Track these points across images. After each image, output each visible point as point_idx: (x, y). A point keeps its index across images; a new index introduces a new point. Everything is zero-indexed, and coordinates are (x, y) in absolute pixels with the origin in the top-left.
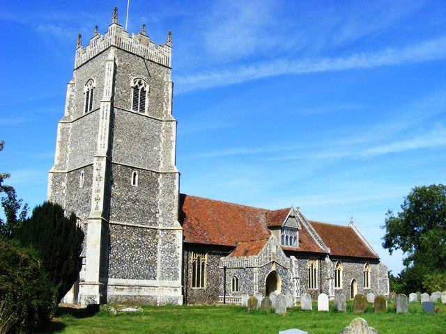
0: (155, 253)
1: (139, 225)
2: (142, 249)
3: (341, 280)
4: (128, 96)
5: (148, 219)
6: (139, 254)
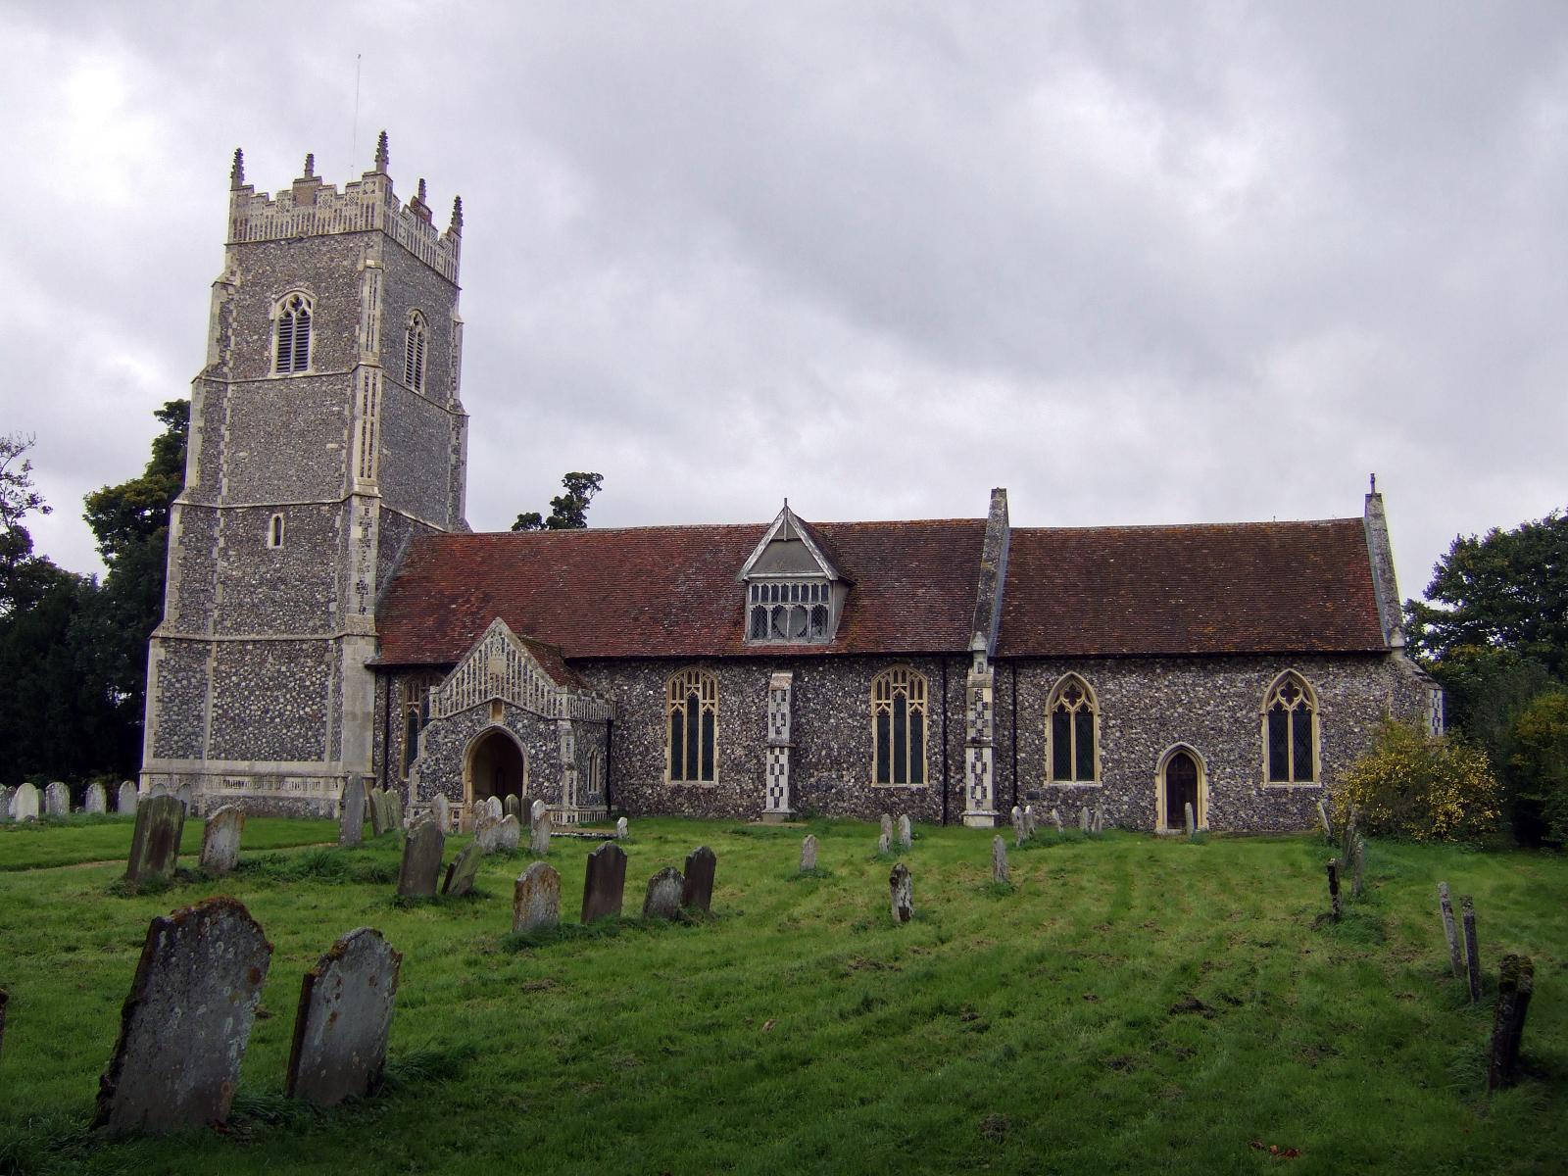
0: (322, 697)
1: (285, 636)
2: (289, 691)
3: (1099, 752)
4: (265, 347)
5: (307, 620)
6: (285, 704)
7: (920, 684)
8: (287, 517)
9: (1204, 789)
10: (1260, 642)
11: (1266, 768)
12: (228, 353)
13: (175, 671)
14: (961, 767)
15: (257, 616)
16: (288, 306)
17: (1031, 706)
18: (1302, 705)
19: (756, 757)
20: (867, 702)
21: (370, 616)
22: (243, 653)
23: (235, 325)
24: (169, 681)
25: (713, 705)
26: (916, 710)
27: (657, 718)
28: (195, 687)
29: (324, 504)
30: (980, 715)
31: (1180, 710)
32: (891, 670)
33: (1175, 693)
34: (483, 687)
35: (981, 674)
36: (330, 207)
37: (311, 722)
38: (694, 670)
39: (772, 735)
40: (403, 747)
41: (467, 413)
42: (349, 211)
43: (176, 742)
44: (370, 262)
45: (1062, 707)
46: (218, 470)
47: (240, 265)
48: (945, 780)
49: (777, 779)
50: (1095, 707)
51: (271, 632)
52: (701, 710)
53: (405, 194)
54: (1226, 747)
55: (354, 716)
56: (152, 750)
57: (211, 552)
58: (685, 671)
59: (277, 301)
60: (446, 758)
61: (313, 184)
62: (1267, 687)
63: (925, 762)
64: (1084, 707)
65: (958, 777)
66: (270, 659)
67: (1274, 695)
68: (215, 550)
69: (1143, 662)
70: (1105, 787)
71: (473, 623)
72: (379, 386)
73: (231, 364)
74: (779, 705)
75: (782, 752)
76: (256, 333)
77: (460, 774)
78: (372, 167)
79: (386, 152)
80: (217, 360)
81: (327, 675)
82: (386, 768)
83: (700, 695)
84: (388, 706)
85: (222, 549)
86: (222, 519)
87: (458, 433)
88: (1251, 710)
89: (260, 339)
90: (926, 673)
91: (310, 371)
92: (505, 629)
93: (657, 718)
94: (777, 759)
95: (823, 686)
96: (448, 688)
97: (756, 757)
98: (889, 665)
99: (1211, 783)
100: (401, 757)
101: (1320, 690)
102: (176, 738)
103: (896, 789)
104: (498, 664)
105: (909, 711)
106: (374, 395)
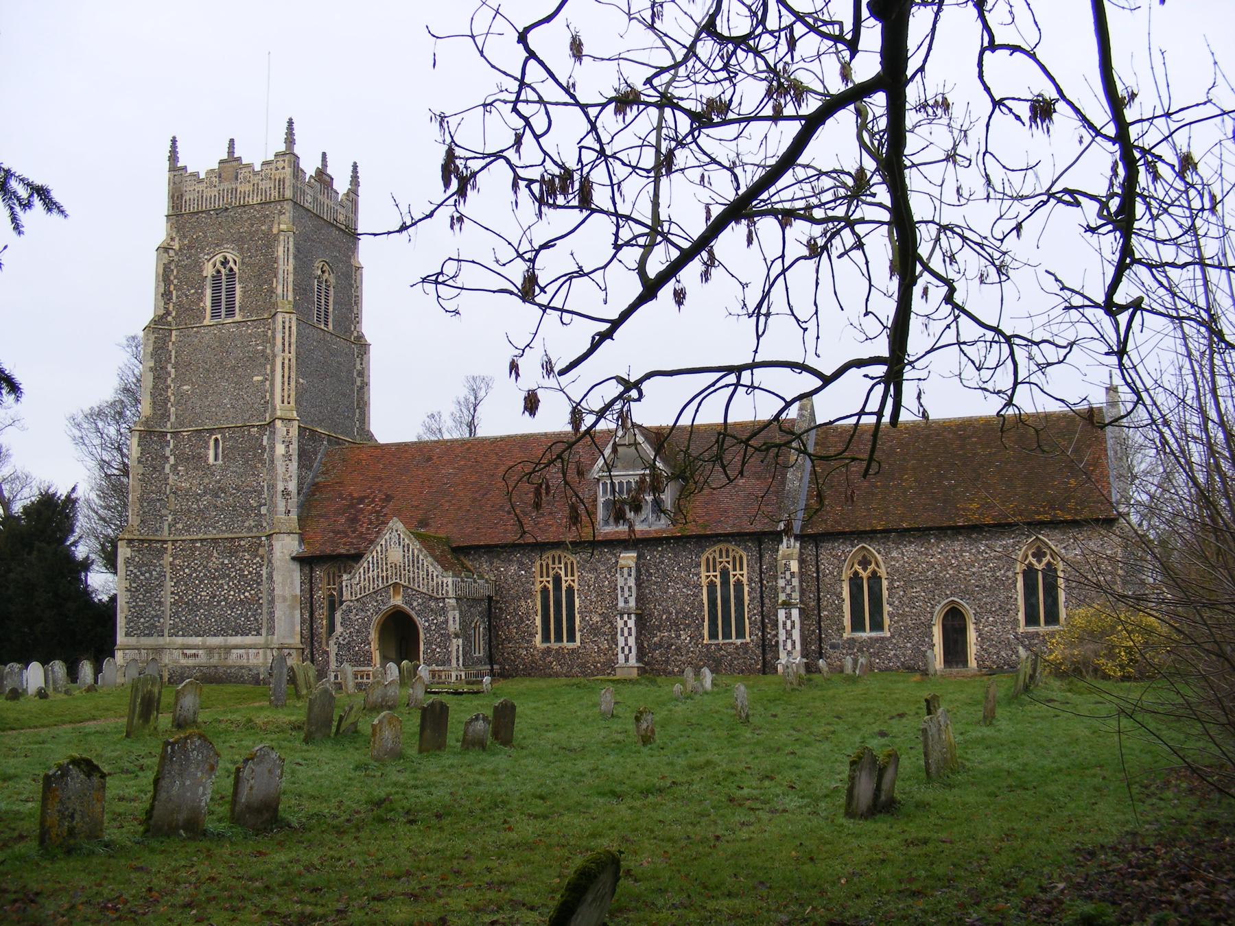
0: (258, 584)
1: (226, 535)
2: (232, 579)
3: (887, 608)
6: (227, 589)
7: (741, 558)
8: (224, 437)
9: (972, 635)
10: (1014, 515)
11: (1021, 616)
12: (171, 304)
13: (138, 567)
14: (776, 625)
15: (204, 519)
16: (218, 264)
17: (831, 573)
18: (1049, 564)
19: (610, 622)
20: (698, 574)
21: (294, 516)
22: (195, 549)
23: (175, 282)
24: (135, 574)
25: (573, 581)
26: (738, 579)
27: (529, 594)
28: (156, 579)
29: (253, 426)
30: (789, 582)
31: (951, 572)
32: (716, 548)
33: (946, 558)
34: (384, 574)
35: (789, 549)
36: (249, 182)
37: (250, 604)
38: (557, 553)
39: (621, 604)
40: (324, 622)
41: (369, 341)
42: (263, 185)
43: (143, 624)
44: (283, 227)
45: (856, 573)
46: (167, 399)
47: (178, 232)
48: (763, 635)
49: (626, 640)
50: (882, 572)
51: (215, 532)
52: (564, 586)
53: (309, 166)
54: (989, 600)
55: (285, 599)
56: (124, 630)
57: (164, 468)
58: (549, 554)
59: (209, 261)
60: (358, 631)
61: (235, 164)
62: (1022, 552)
63: (747, 621)
64: (874, 573)
65: (774, 632)
66: (215, 554)
67: (1027, 557)
68: (167, 467)
69: (919, 533)
70: (892, 636)
71: (377, 519)
72: (294, 328)
73: (174, 314)
74: (626, 579)
75: (629, 618)
76: (193, 287)
77: (370, 644)
78: (282, 147)
79: (292, 129)
80: (162, 312)
81: (261, 566)
82: (312, 639)
83: (562, 573)
84: (311, 590)
85: (172, 466)
86: (172, 441)
87: (362, 359)
88: (1008, 570)
89: (196, 292)
90: (745, 549)
91: (238, 318)
92: (400, 526)
93: (529, 594)
94: (626, 623)
95: (662, 562)
96: (357, 576)
97: (610, 622)
98: (715, 544)
99: (977, 630)
100: (323, 631)
101: (1063, 551)
102: (142, 620)
103: (724, 644)
104: (396, 555)
105: (732, 580)
106: (290, 336)
